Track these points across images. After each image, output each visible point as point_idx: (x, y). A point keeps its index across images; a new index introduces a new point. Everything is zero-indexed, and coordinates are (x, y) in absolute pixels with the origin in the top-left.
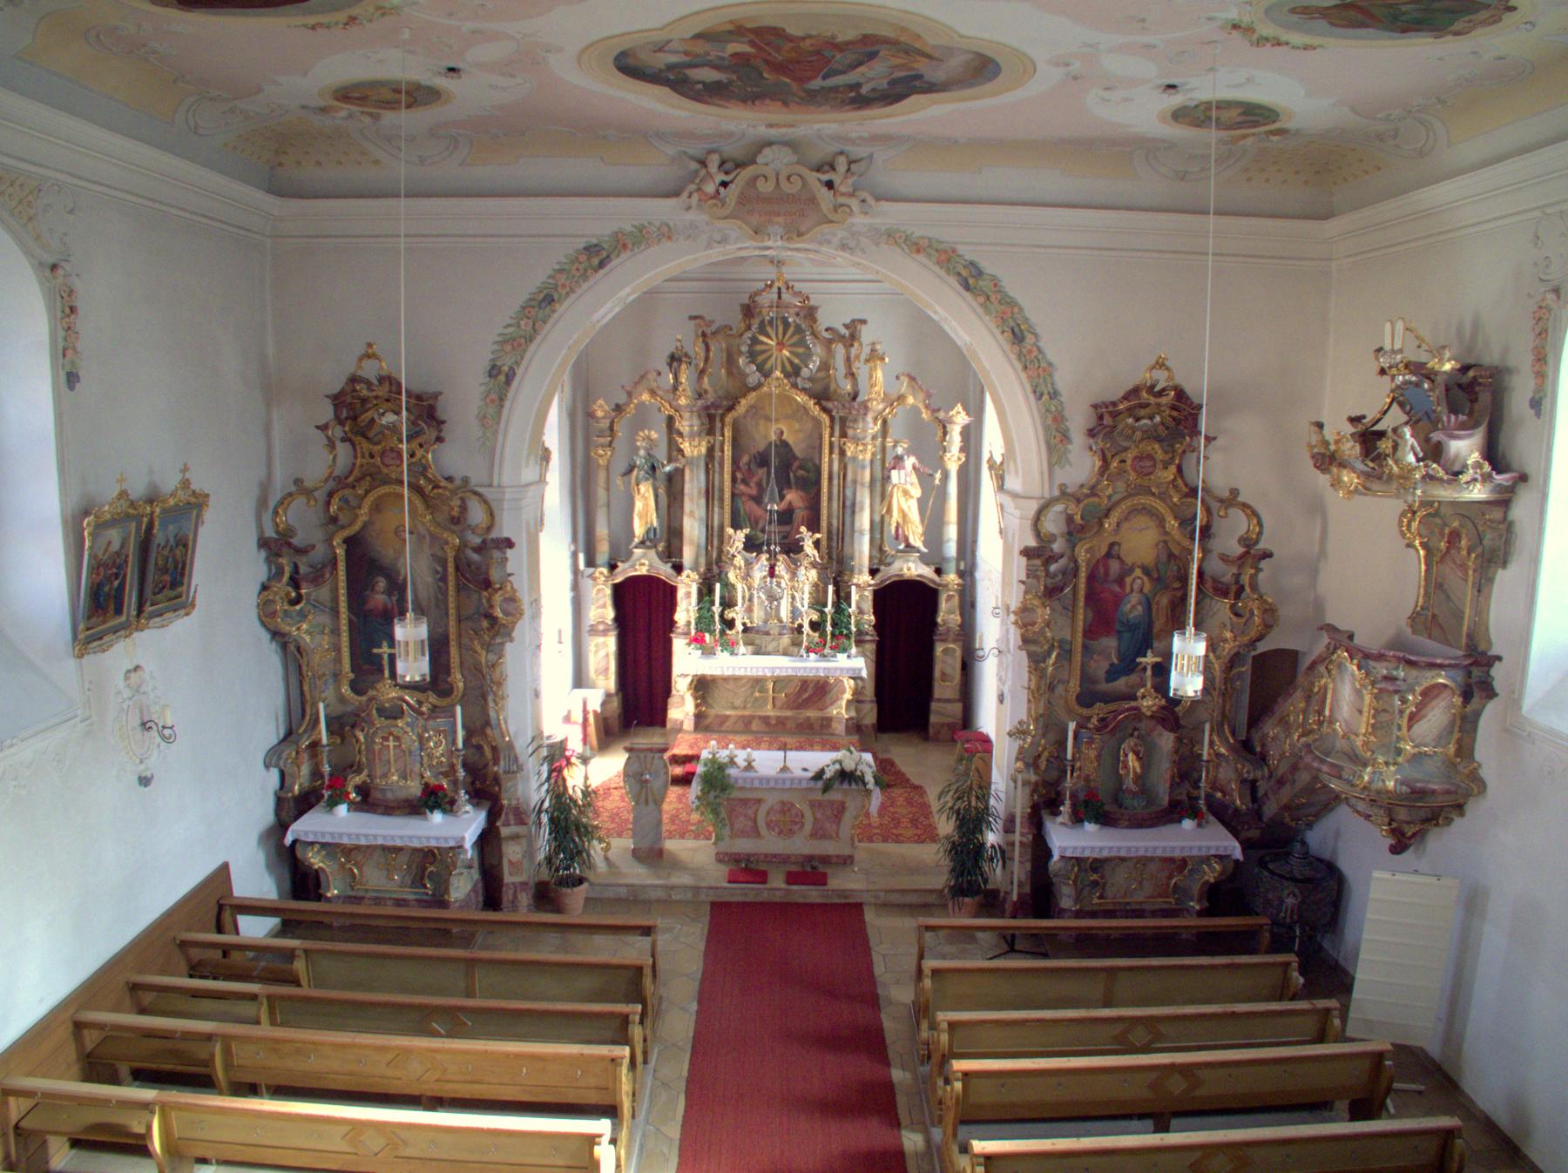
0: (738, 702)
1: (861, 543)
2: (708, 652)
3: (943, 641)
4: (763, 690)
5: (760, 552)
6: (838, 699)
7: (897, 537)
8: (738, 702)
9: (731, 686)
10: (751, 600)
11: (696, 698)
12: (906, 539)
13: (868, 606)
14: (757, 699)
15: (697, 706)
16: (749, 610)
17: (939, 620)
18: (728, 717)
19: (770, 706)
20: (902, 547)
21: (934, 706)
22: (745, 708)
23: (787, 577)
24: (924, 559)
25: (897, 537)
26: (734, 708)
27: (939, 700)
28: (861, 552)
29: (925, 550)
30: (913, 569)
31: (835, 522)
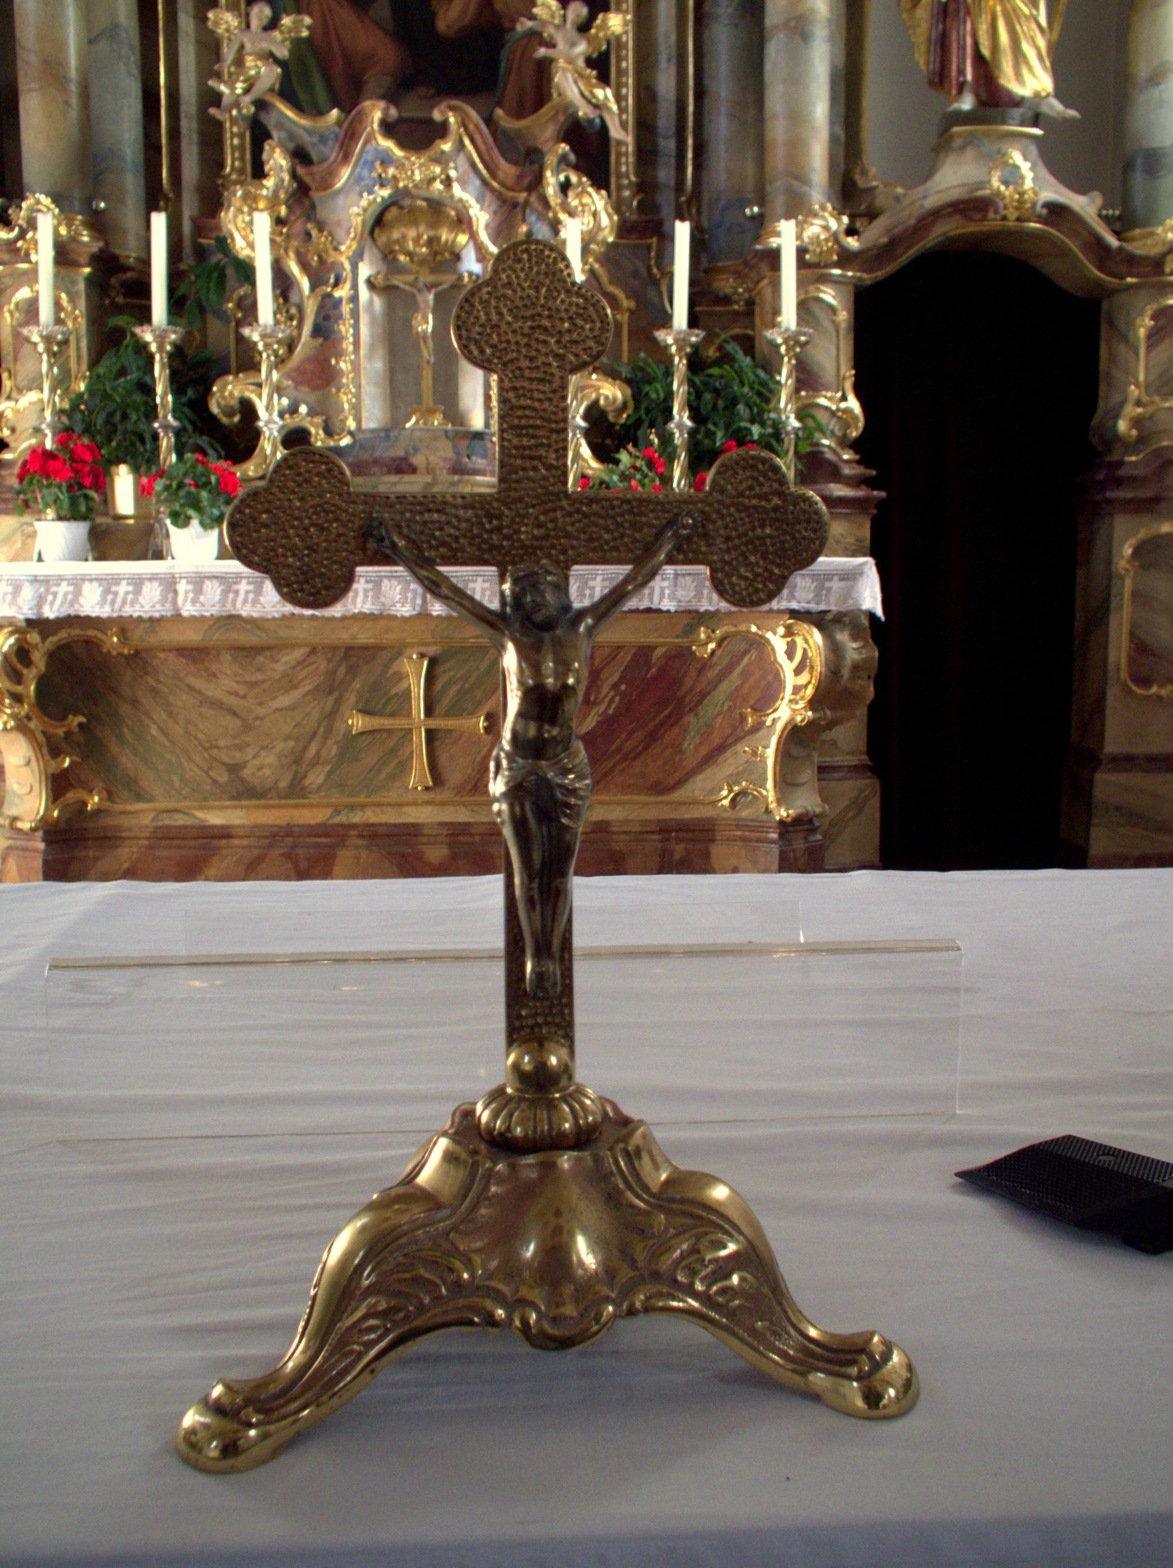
0: (264, 765)
1: (797, 79)
2: (107, 540)
3: (1149, 506)
4: (383, 700)
5: (348, 97)
6: (738, 732)
7: (940, 78)
8: (264, 765)
9: (225, 682)
10: (324, 329)
11: (52, 748)
12: (986, 69)
13: (834, 356)
14: (352, 744)
15: (58, 785)
16: (319, 376)
17: (1122, 426)
18: (224, 833)
19: (418, 775)
20: (967, 104)
21: (1107, 785)
22: (296, 790)
23: (481, 217)
24: (1057, 155)
25: (940, 78)
26: (247, 792)
27: (1125, 762)
28: (797, 116)
29: (1072, 113)
30: (1023, 177)
31: (665, 83)
